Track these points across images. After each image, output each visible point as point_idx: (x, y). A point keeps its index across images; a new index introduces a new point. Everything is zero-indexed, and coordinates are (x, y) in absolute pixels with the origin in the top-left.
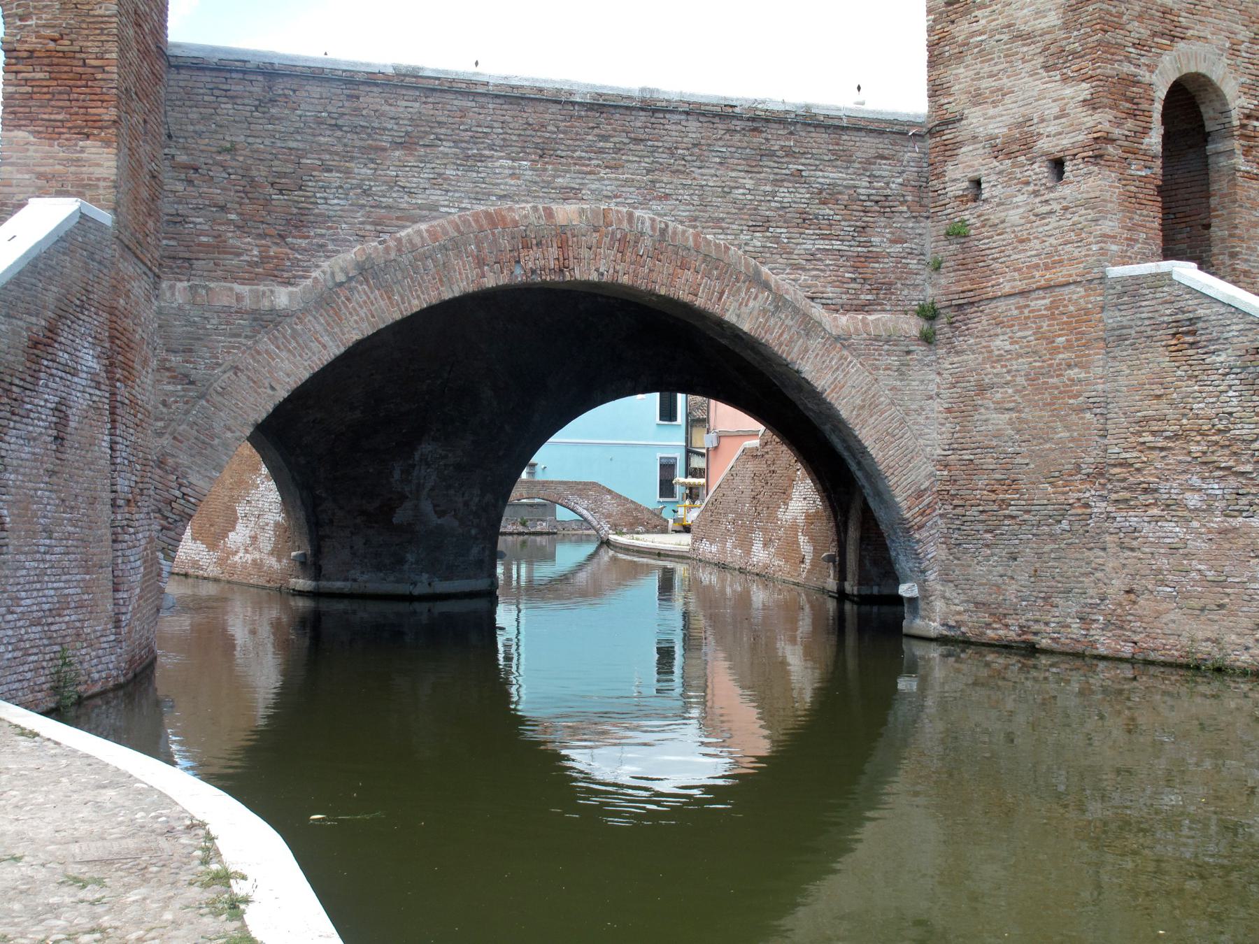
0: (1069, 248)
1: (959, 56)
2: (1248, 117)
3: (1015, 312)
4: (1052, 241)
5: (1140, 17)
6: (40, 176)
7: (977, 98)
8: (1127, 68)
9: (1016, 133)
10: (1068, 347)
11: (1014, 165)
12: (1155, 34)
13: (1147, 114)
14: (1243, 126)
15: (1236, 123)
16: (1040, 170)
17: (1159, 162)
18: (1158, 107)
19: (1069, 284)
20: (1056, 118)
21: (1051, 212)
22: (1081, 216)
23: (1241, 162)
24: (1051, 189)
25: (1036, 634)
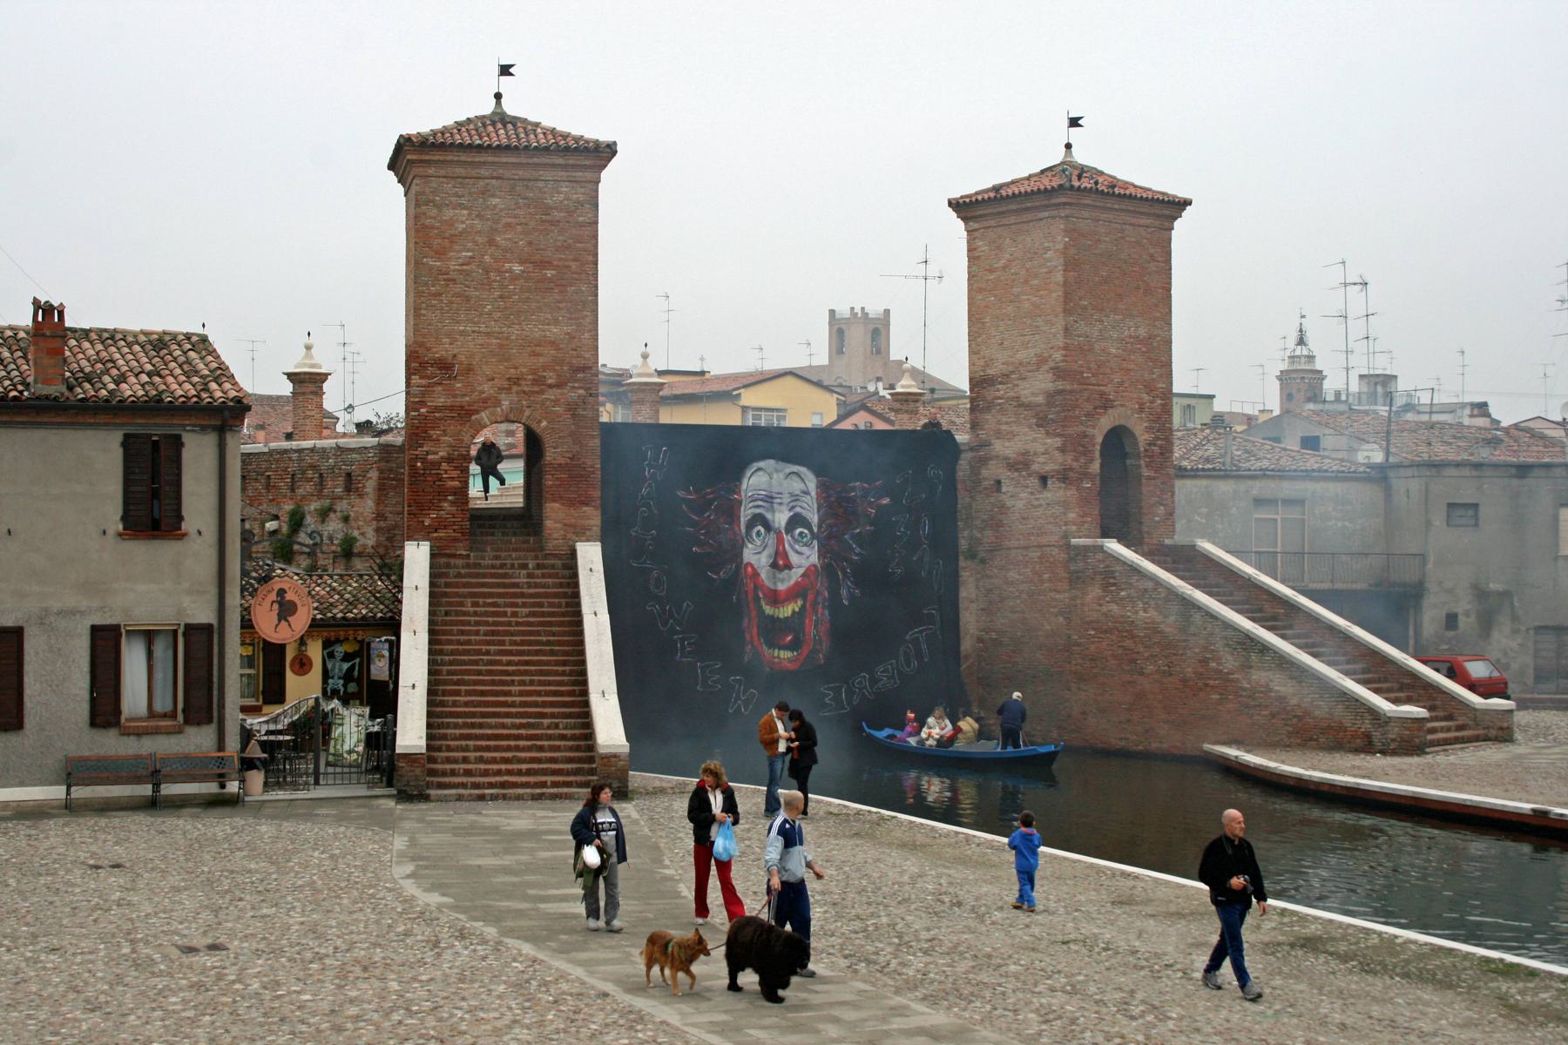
0: (1050, 526)
1: (988, 409)
2: (1150, 444)
3: (1021, 558)
4: (1041, 521)
5: (1088, 400)
6: (565, 525)
7: (999, 434)
8: (1081, 428)
9: (1021, 458)
10: (1050, 580)
11: (1020, 476)
12: (1095, 408)
13: (1091, 452)
14: (1146, 450)
15: (1142, 449)
16: (1035, 482)
17: (1098, 478)
18: (1098, 447)
19: (1049, 546)
20: (1043, 454)
21: (1040, 505)
22: (1058, 510)
23: (1146, 472)
24: (1040, 492)
25: (1034, 736)
